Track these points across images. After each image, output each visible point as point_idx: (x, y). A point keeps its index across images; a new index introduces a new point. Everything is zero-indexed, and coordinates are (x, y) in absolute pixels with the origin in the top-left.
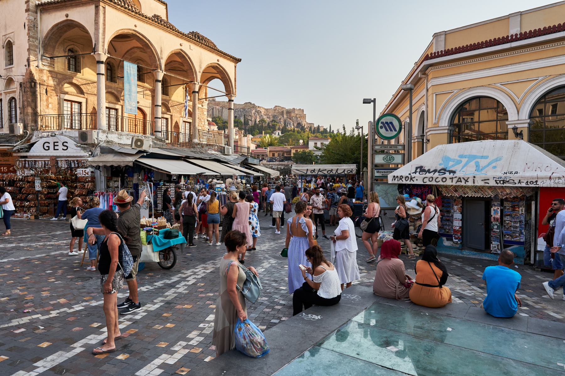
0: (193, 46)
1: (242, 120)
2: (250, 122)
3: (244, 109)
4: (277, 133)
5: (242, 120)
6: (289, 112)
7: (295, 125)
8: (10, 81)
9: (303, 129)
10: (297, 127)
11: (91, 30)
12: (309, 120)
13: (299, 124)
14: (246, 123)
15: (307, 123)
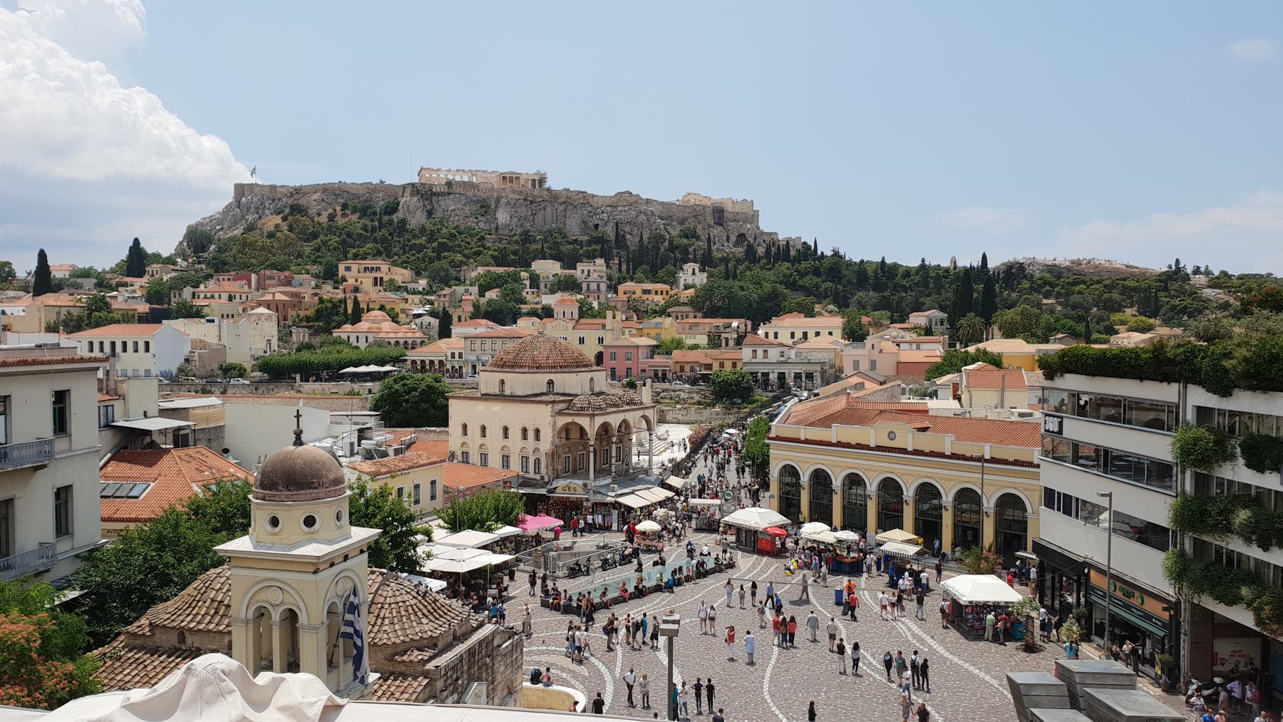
0: (631, 414)
1: (610, 232)
2: (628, 237)
3: (614, 206)
4: (690, 271)
5: (612, 236)
6: (719, 214)
7: (733, 238)
8: (536, 450)
9: (750, 251)
10: (737, 244)
11: (588, 429)
12: (766, 225)
13: (742, 237)
14: (620, 240)
15: (762, 233)
